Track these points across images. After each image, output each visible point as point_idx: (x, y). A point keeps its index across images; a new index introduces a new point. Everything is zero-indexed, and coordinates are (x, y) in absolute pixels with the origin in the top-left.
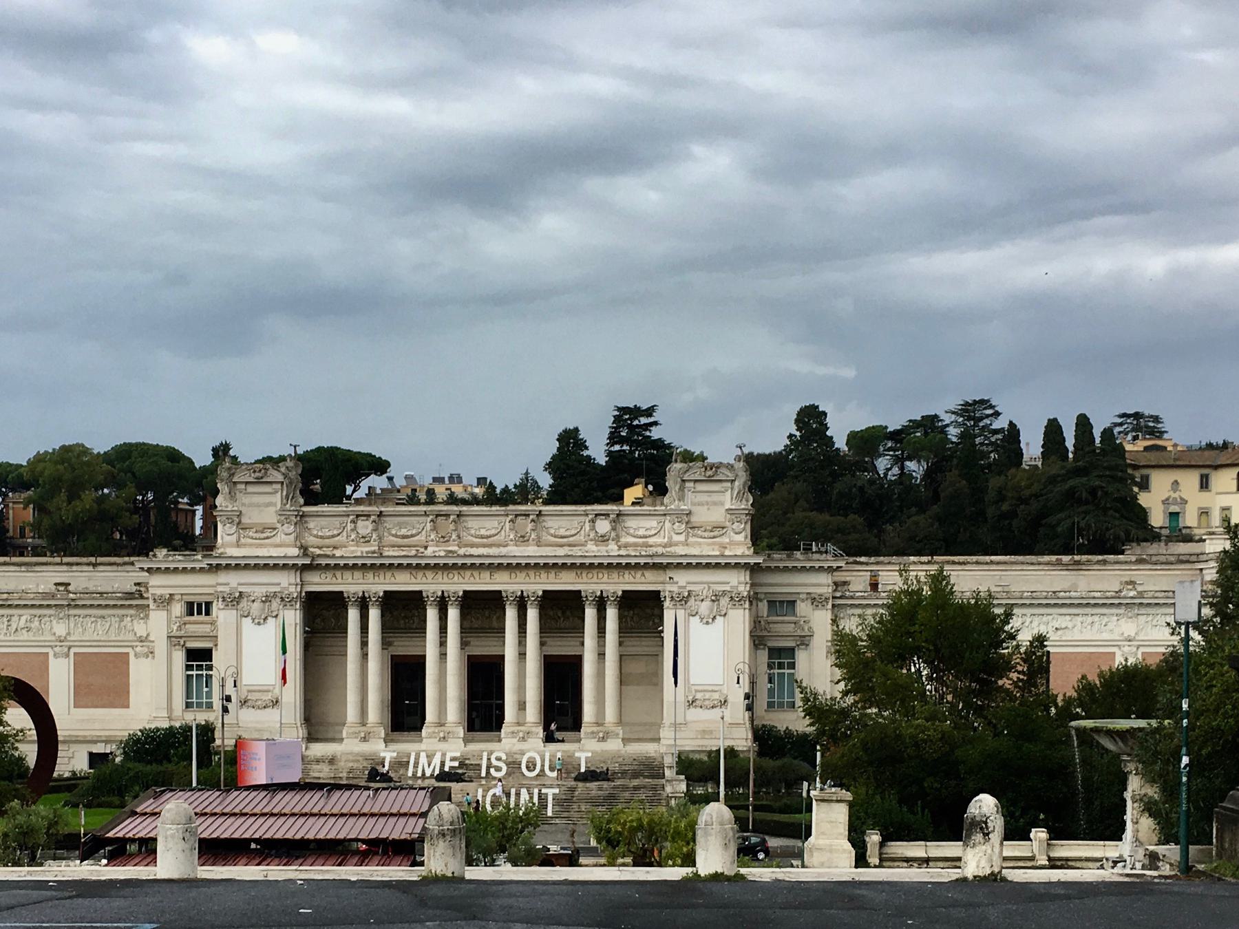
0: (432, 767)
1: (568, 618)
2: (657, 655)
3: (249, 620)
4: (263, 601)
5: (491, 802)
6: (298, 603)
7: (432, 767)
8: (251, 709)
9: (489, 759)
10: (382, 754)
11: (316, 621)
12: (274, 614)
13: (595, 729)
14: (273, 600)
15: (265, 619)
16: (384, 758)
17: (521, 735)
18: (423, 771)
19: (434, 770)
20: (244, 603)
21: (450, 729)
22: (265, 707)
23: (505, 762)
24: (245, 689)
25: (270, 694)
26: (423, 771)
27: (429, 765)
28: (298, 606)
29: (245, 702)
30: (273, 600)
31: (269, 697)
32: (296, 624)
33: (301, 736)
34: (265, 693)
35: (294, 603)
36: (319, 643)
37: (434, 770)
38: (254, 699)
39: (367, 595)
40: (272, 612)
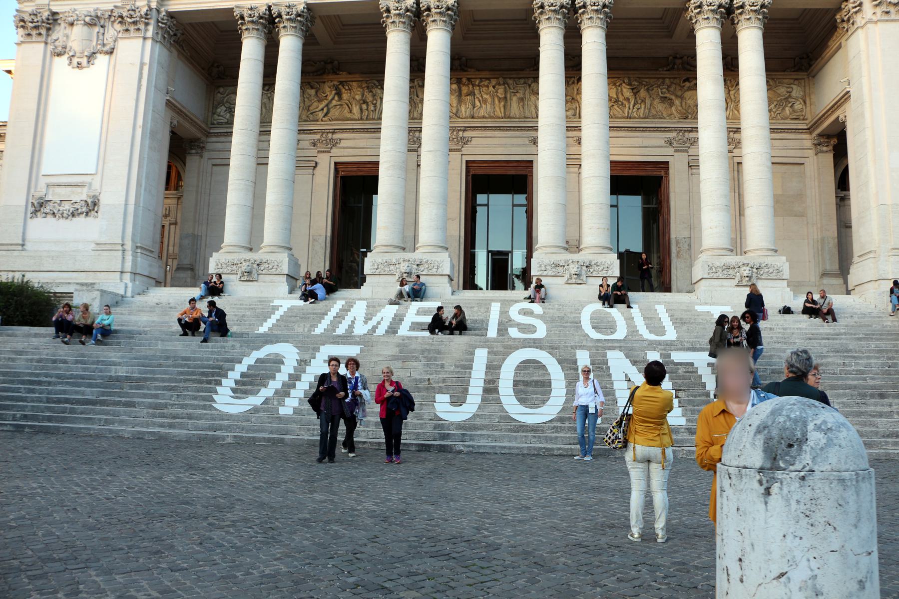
0: (371, 324)
1: (643, 101)
2: (803, 164)
3: (64, 59)
4: (87, 24)
5: (516, 383)
6: (151, 28)
7: (371, 324)
8: (50, 219)
9: (504, 313)
10: (276, 303)
11: (219, 110)
12: (107, 48)
13: (732, 259)
14: (108, 25)
15: (91, 57)
16: (276, 308)
17: (573, 269)
18: (351, 327)
19: (374, 329)
20: (59, 33)
21: (425, 257)
22: (73, 215)
23: (538, 317)
24: (43, 182)
25: (85, 190)
26: (351, 327)
27: (367, 319)
28: (150, 34)
29: (41, 205)
30: (108, 25)
31: (81, 195)
32: (142, 65)
33: (128, 266)
34: (79, 189)
35: (142, 26)
36: (219, 146)
37: (374, 329)
38: (57, 199)
39: (275, 11)
40: (104, 45)
